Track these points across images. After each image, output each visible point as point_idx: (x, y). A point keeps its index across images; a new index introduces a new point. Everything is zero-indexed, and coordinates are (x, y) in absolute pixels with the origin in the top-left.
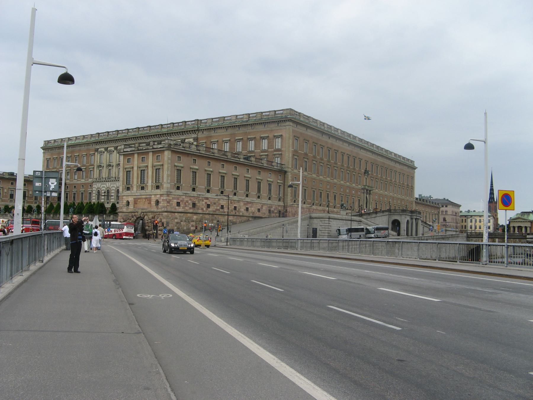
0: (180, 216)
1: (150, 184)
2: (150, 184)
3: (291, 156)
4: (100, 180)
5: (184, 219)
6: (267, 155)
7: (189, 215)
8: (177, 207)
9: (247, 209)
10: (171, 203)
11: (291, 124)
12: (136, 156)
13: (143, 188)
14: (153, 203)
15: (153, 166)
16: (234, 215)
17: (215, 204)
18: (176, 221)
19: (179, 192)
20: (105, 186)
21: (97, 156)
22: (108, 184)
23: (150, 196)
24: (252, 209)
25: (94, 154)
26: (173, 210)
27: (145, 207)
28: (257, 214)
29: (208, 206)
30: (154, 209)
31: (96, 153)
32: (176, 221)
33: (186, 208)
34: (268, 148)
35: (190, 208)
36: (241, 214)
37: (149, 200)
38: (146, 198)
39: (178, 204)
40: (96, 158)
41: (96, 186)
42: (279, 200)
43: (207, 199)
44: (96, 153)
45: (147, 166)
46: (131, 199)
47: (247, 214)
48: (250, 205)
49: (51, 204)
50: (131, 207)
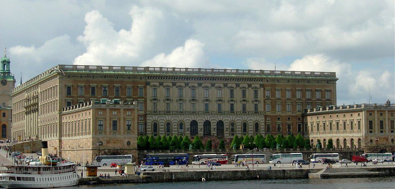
1: (387, 128)
2: (387, 128)
4: (155, 113)
6: (321, 103)
12: (376, 112)
13: (382, 132)
14: (390, 141)
15: (389, 119)
20: (164, 119)
21: (150, 90)
22: (168, 118)
23: (388, 137)
25: (145, 87)
27: (384, 143)
30: (391, 144)
31: (148, 87)
37: (387, 139)
38: (384, 138)
40: (148, 91)
41: (150, 119)
44: (148, 87)
45: (385, 120)
46: (373, 138)
49: (187, 136)
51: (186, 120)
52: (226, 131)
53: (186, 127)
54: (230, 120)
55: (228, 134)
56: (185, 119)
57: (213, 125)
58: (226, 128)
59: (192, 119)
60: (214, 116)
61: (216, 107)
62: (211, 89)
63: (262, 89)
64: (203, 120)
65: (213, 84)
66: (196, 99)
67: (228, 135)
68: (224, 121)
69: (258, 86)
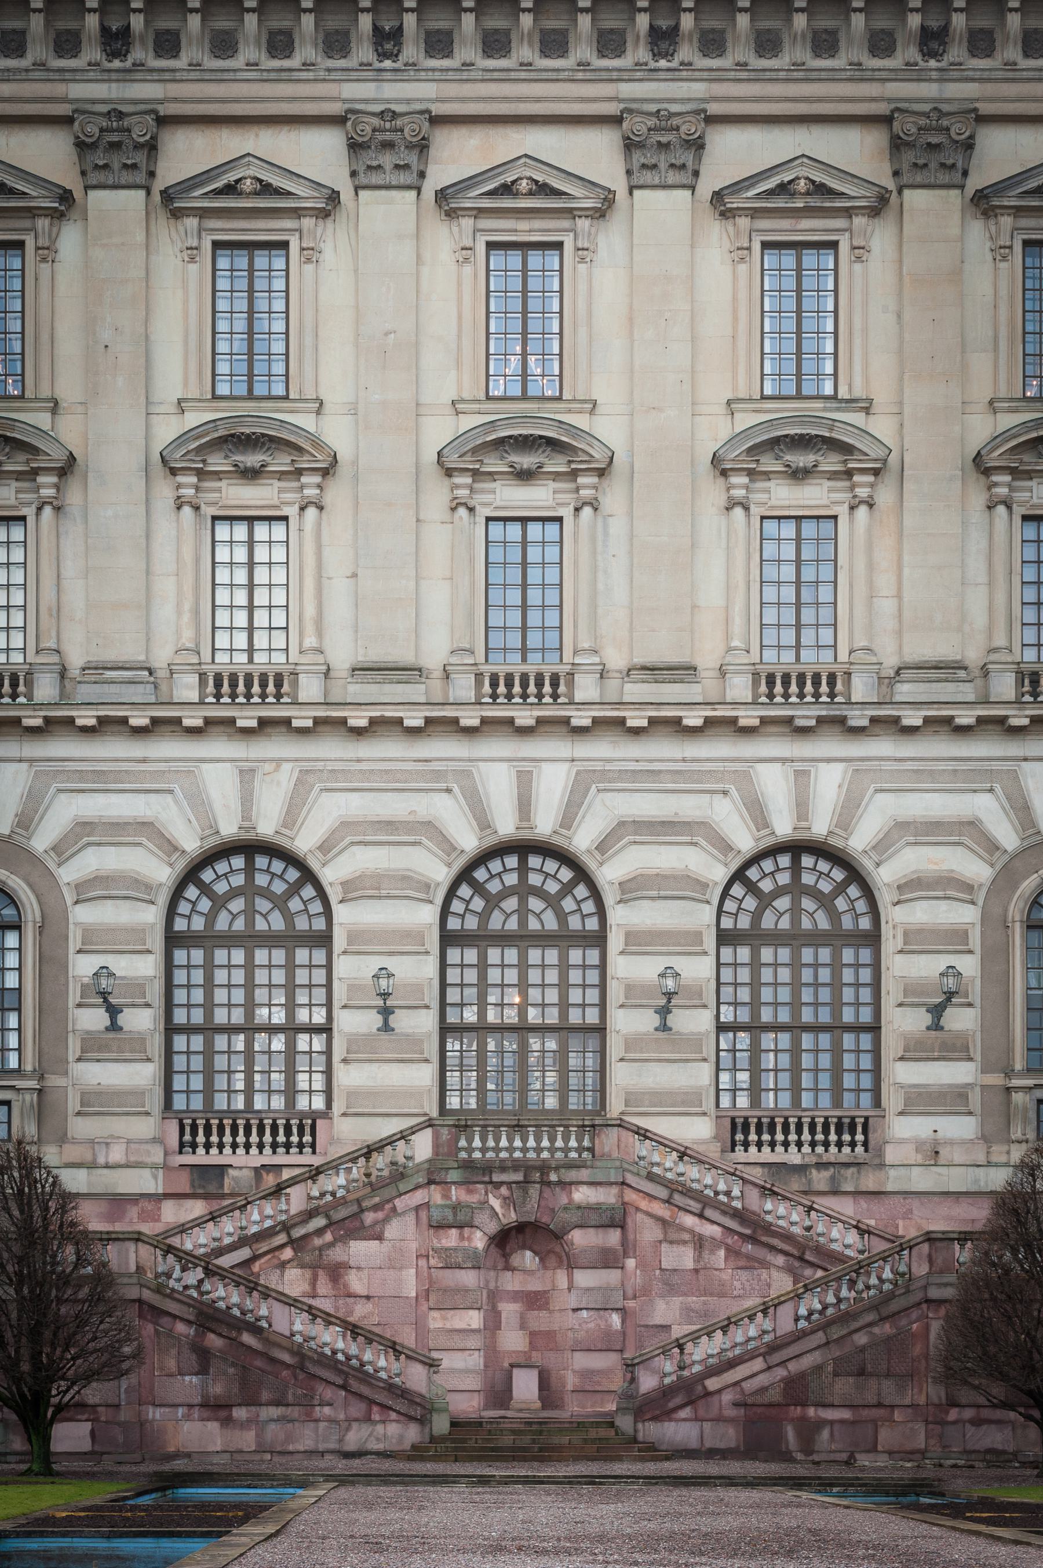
51: (85, 833)
52: (915, 1052)
53: (84, 967)
54: (1009, 839)
55: (952, 1101)
56: (64, 812)
57: (639, 942)
58: (912, 992)
59: (199, 803)
60: (663, 750)
61: (711, 593)
62: (610, 240)
64: (430, 830)
65: (664, 120)
66: (306, 421)
67: (960, 1128)
68: (883, 846)
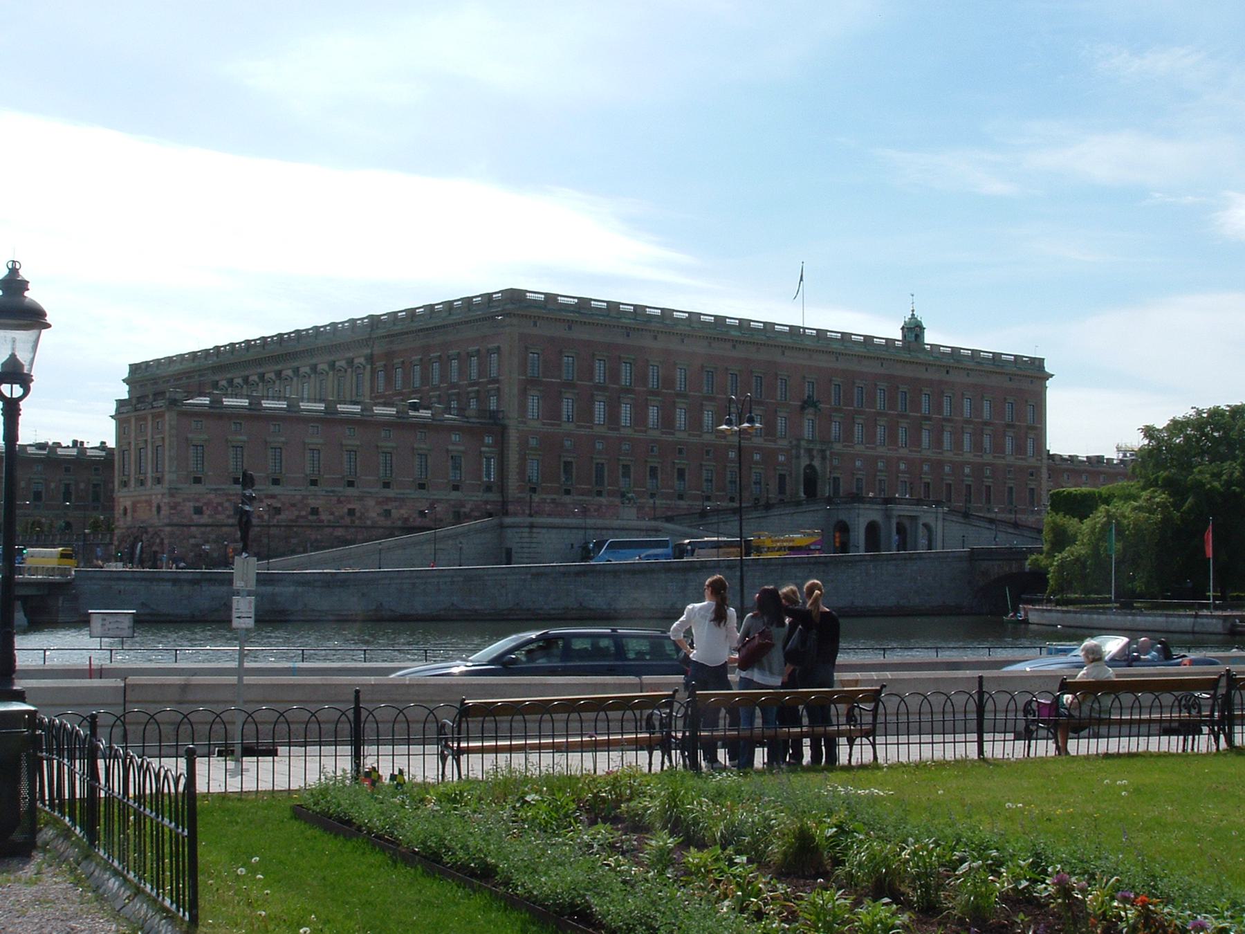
0: (203, 533)
3: (515, 391)
5: (213, 536)
7: (225, 529)
8: (195, 517)
9: (387, 513)
10: (179, 508)
11: (515, 321)
16: (347, 527)
17: (293, 505)
18: (192, 541)
19: (198, 488)
24: (402, 511)
26: (185, 521)
28: (419, 522)
29: (278, 511)
32: (192, 541)
33: (218, 516)
34: (480, 377)
35: (229, 517)
36: (369, 523)
39: (198, 511)
42: (488, 488)
43: (273, 497)
47: (389, 523)
48: (395, 504)
50: (129, 518)
63: (369, 367)
69: (362, 360)
